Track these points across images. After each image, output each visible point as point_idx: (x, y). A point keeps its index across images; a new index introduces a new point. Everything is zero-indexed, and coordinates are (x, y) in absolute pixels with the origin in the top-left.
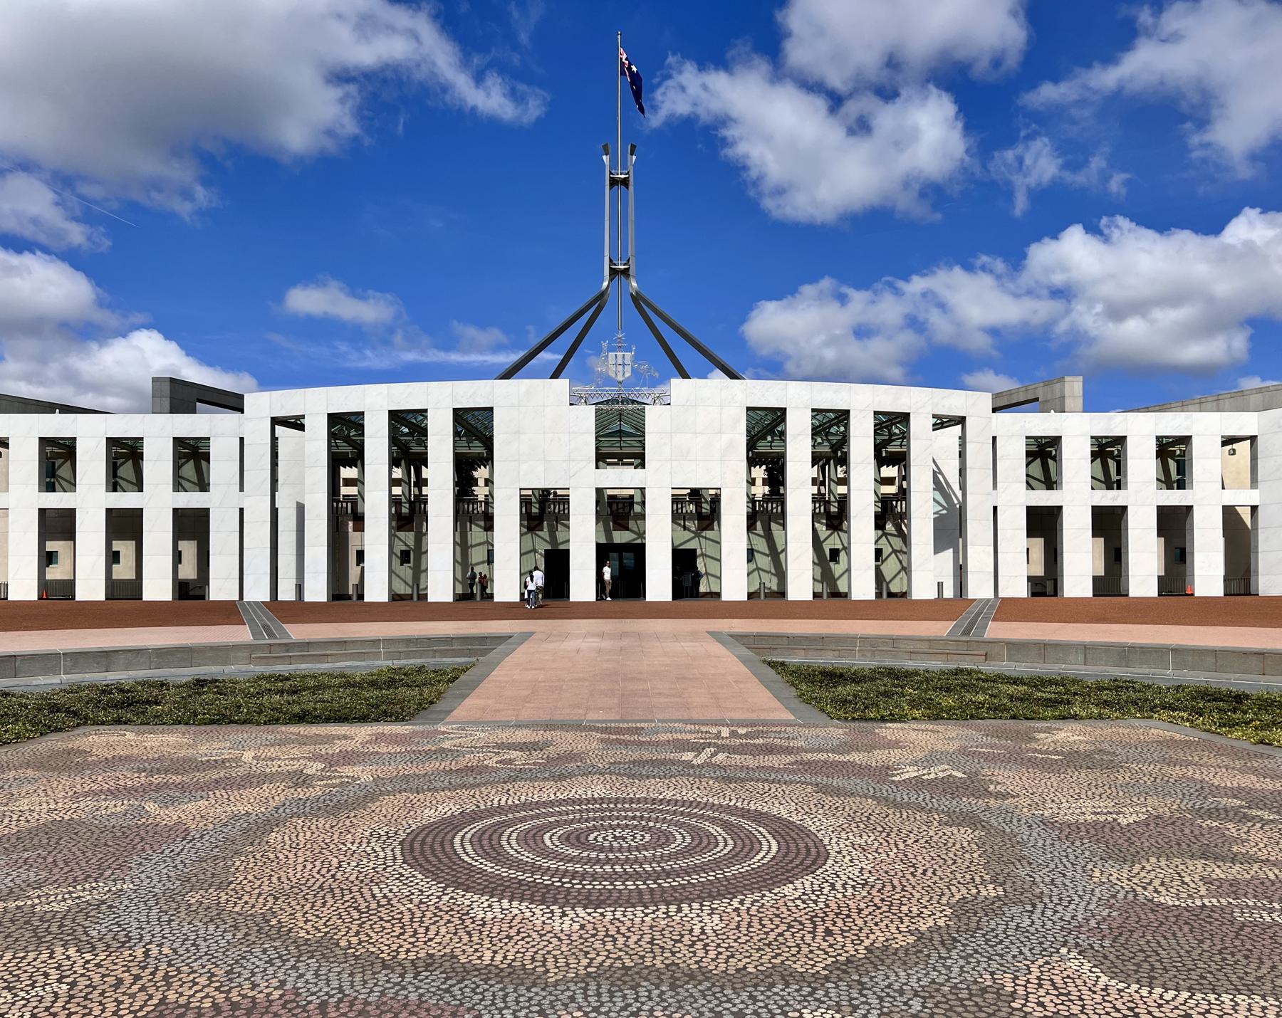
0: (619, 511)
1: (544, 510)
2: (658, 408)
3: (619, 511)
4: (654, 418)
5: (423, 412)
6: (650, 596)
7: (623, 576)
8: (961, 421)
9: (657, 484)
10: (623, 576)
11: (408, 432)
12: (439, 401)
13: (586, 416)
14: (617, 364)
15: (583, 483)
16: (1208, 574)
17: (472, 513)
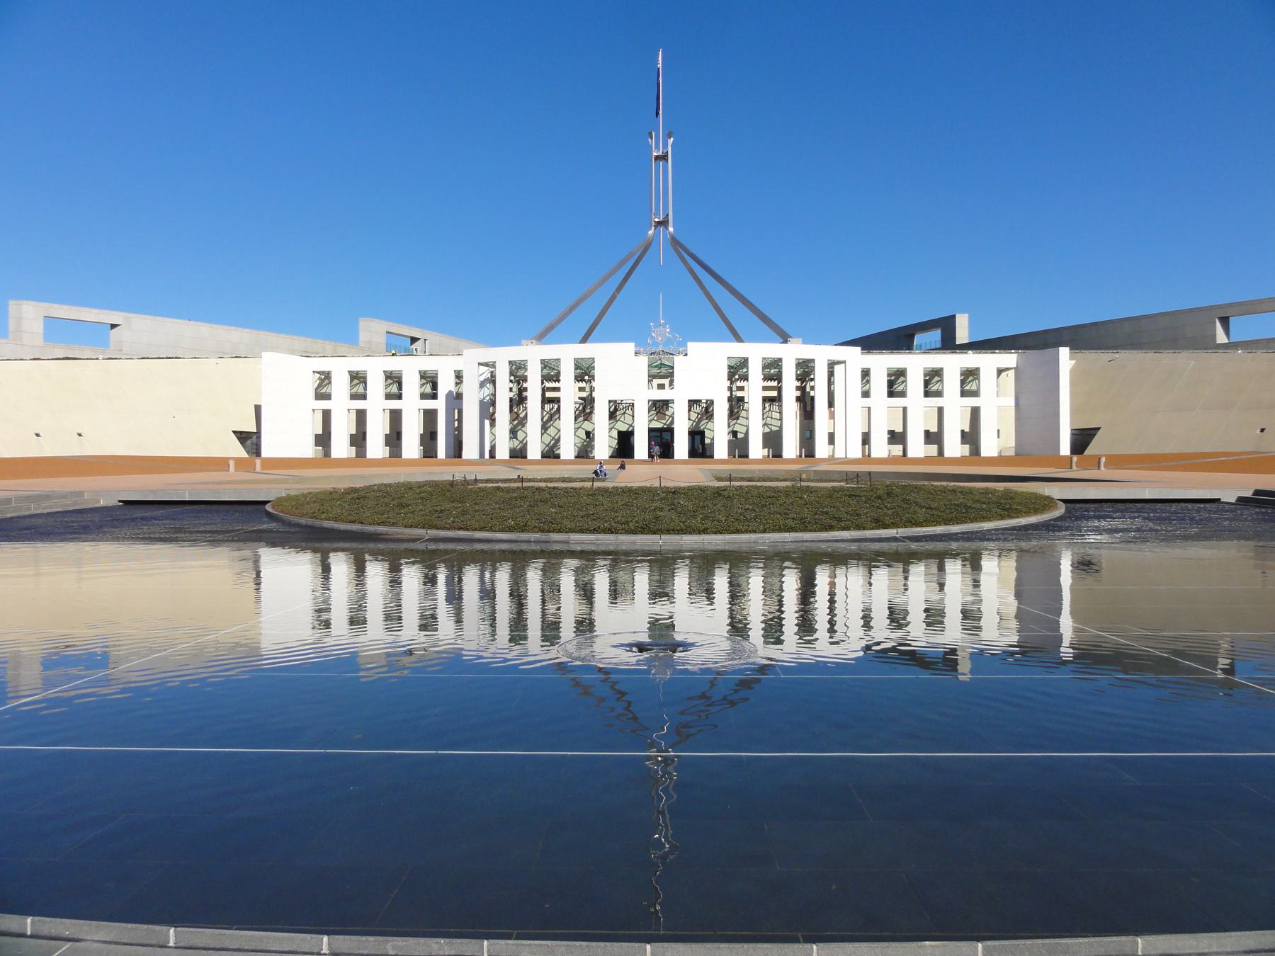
0: (660, 407)
2: (681, 357)
3: (660, 407)
4: (679, 362)
5: (558, 360)
6: (676, 457)
7: (662, 442)
8: (844, 362)
9: (679, 396)
10: (662, 442)
11: (551, 373)
12: (567, 354)
13: (643, 361)
14: (662, 334)
15: (641, 394)
17: (586, 408)
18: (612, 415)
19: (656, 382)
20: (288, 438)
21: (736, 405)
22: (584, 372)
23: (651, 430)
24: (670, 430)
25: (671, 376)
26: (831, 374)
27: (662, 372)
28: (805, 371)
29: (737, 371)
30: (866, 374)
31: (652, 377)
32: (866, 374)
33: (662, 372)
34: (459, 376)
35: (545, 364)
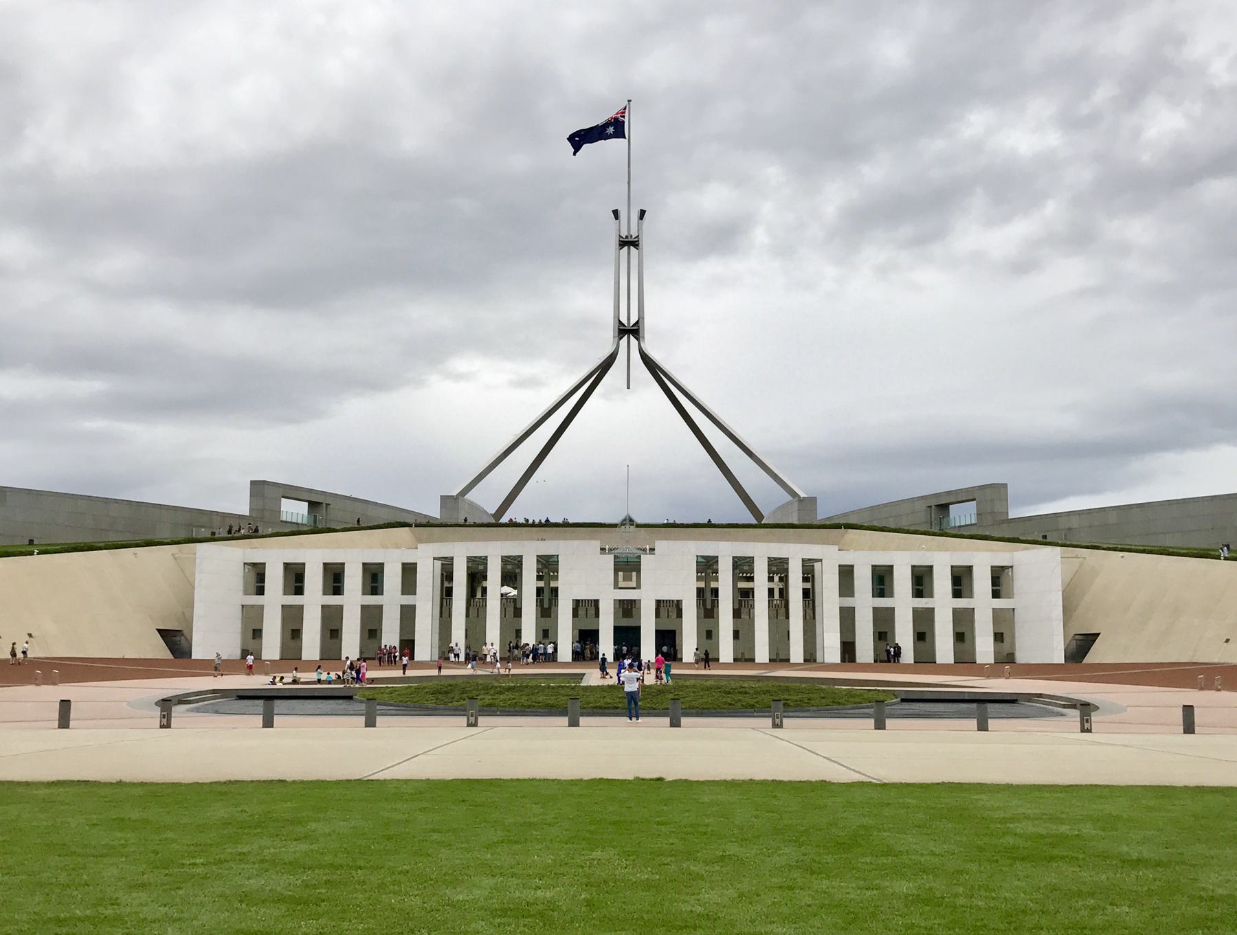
1: (586, 608)
16: (984, 649)
18: (575, 614)
19: (621, 574)
20: (213, 637)
21: (707, 601)
22: (548, 566)
23: (616, 629)
24: (637, 630)
25: (639, 571)
26: (809, 574)
27: (627, 567)
28: (778, 568)
29: (707, 566)
30: (846, 573)
31: (616, 571)
32: (846, 573)
33: (627, 567)
34: (409, 570)
35: (505, 560)
